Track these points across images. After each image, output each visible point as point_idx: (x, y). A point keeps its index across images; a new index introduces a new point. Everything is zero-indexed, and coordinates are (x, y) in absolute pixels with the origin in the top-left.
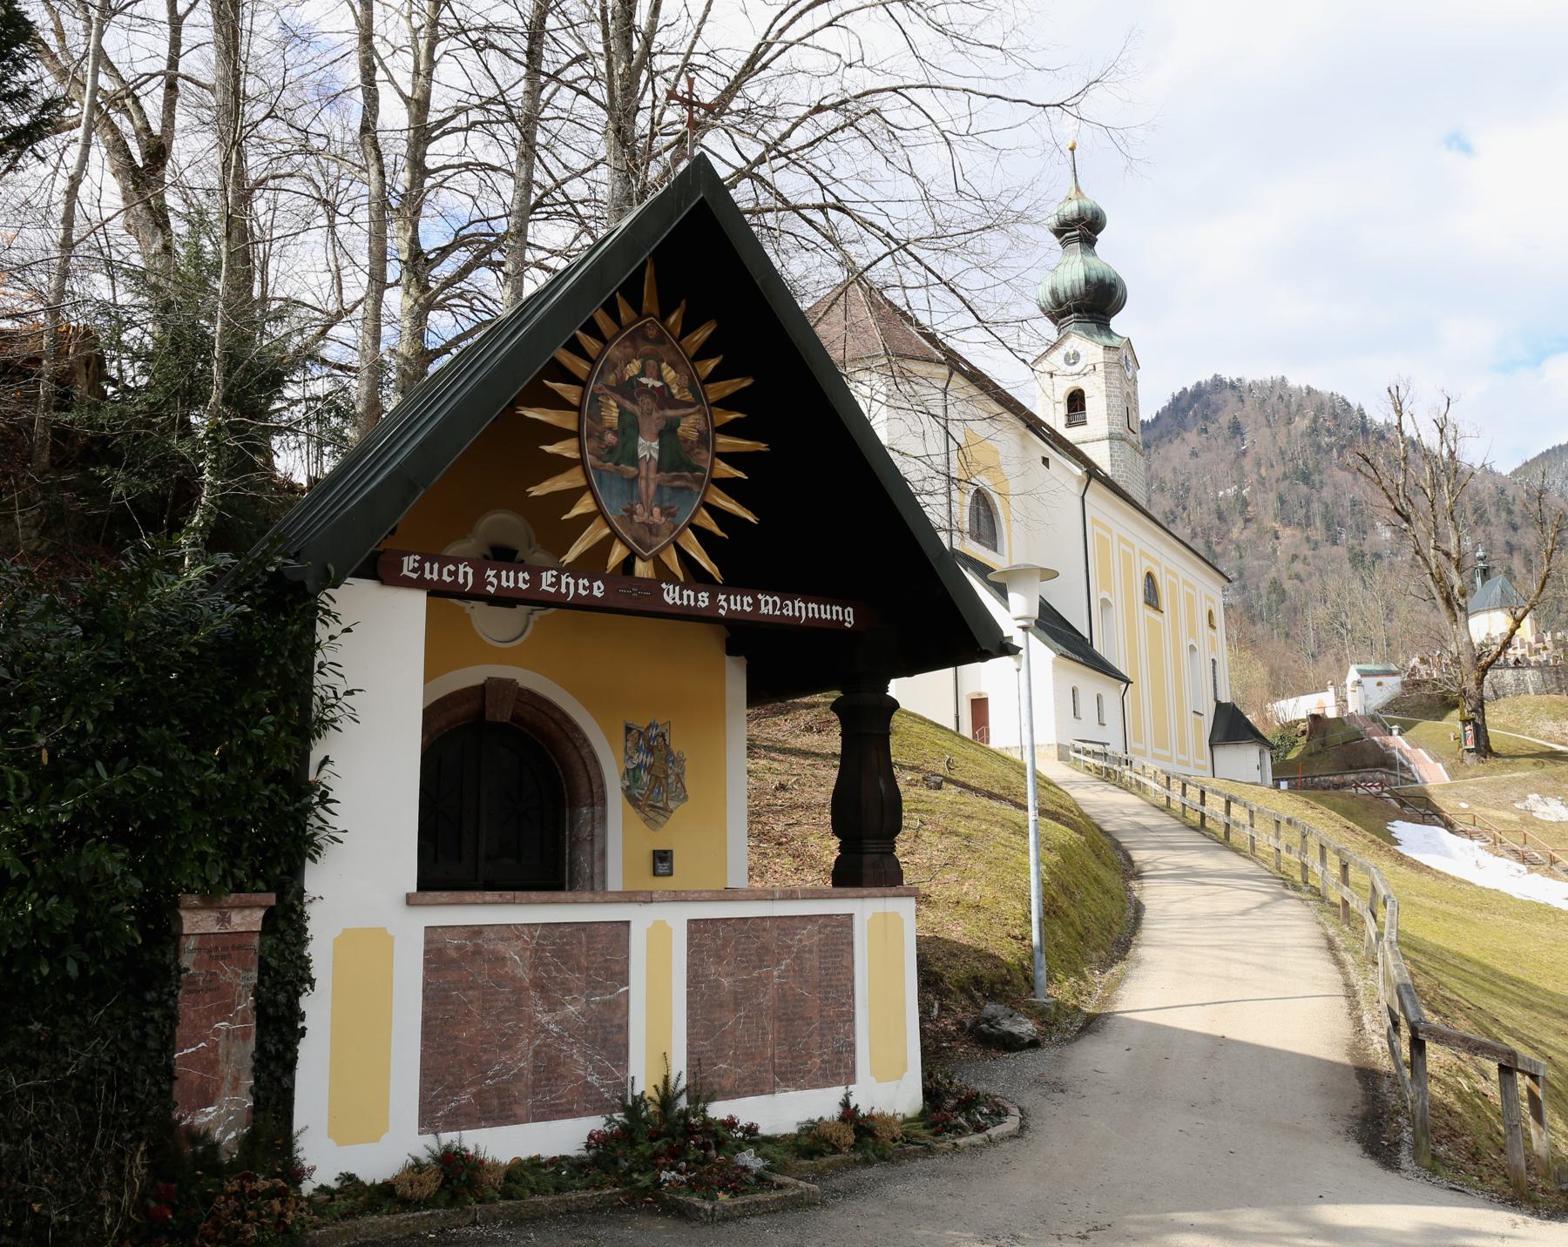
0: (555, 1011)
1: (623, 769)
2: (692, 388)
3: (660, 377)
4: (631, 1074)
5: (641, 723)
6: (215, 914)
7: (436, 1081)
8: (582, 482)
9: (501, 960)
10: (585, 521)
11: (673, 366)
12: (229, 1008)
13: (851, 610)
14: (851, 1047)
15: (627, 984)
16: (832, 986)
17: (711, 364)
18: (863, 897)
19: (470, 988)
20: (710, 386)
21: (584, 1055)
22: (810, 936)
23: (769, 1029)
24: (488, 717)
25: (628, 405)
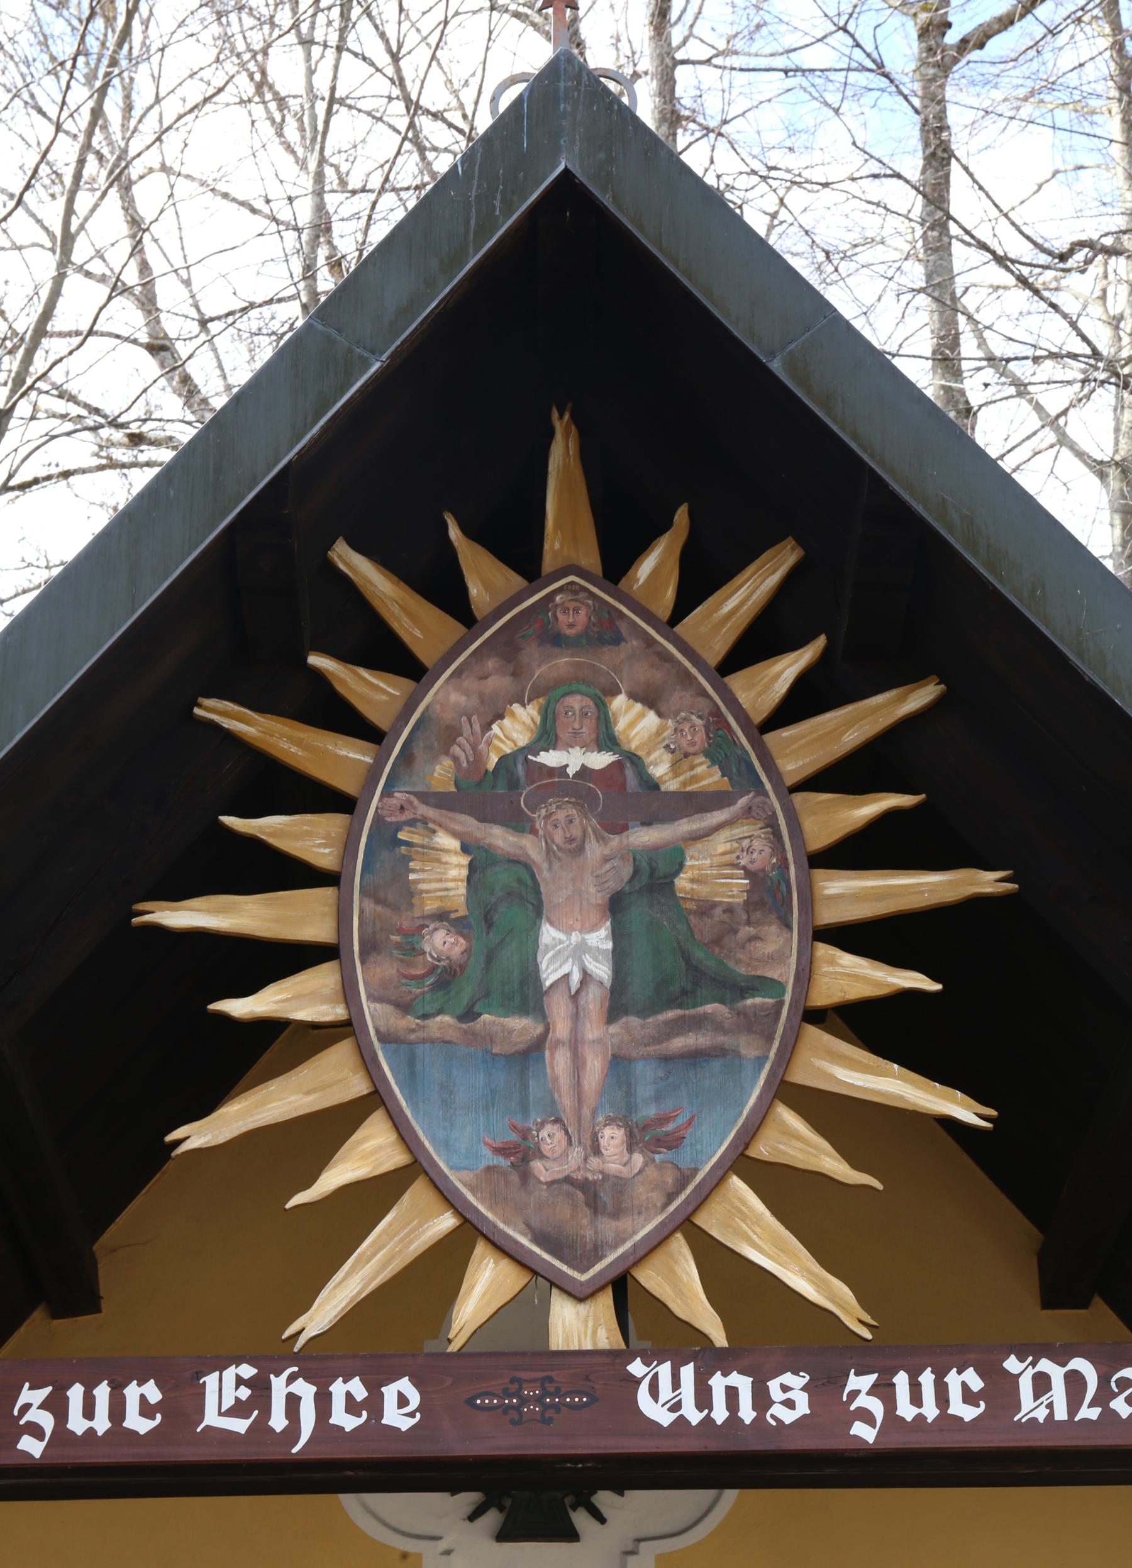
3: (606, 739)
8: (357, 1086)
11: (649, 699)
20: (787, 733)
25: (500, 838)
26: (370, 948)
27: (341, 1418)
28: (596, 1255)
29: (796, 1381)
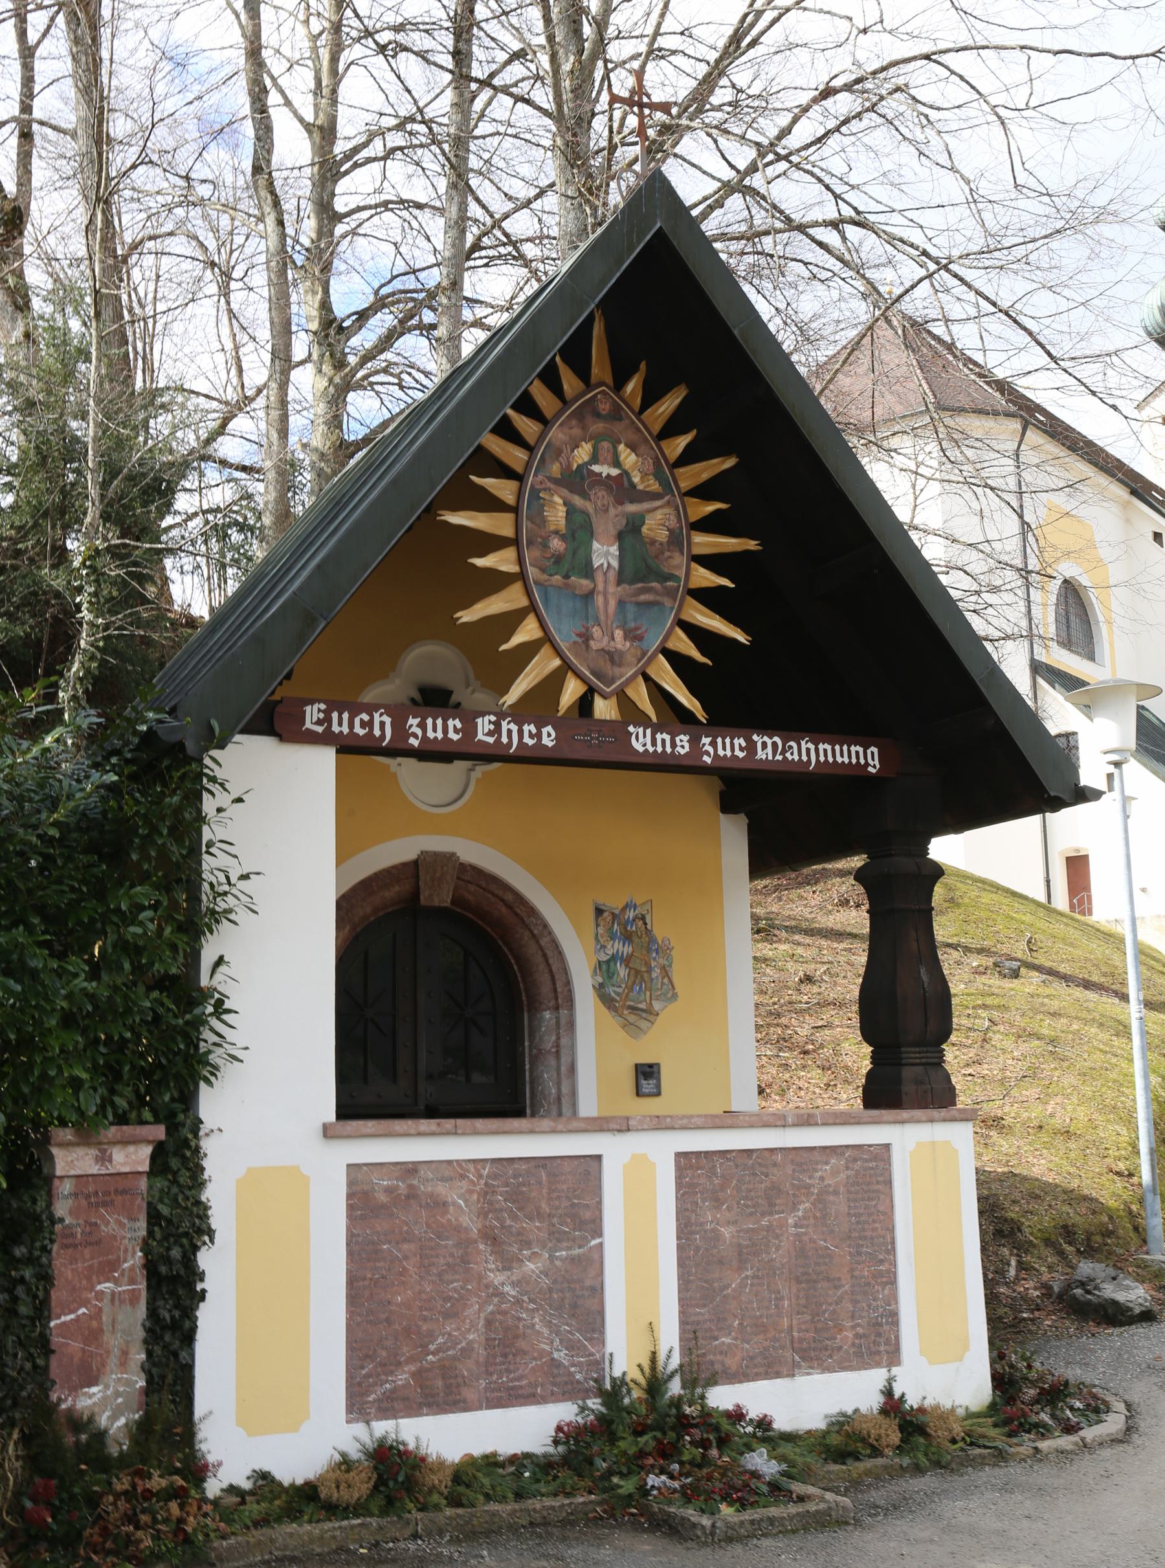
0: (509, 1269)
1: (594, 961)
2: (658, 475)
3: (617, 463)
4: (609, 1348)
5: (614, 902)
6: (93, 1152)
7: (367, 1356)
8: (524, 602)
9: (440, 1205)
10: (529, 650)
11: (633, 447)
12: (114, 1265)
13: (875, 750)
14: (893, 1318)
15: (601, 1235)
16: (865, 1238)
17: (681, 443)
18: (903, 1122)
19: (405, 1240)
20: (682, 470)
21: (549, 1324)
22: (835, 1172)
23: (785, 1292)
24: (423, 901)
25: (578, 501)
26: (530, 543)
27: (527, 740)
28: (613, 681)
29: (685, 738)
